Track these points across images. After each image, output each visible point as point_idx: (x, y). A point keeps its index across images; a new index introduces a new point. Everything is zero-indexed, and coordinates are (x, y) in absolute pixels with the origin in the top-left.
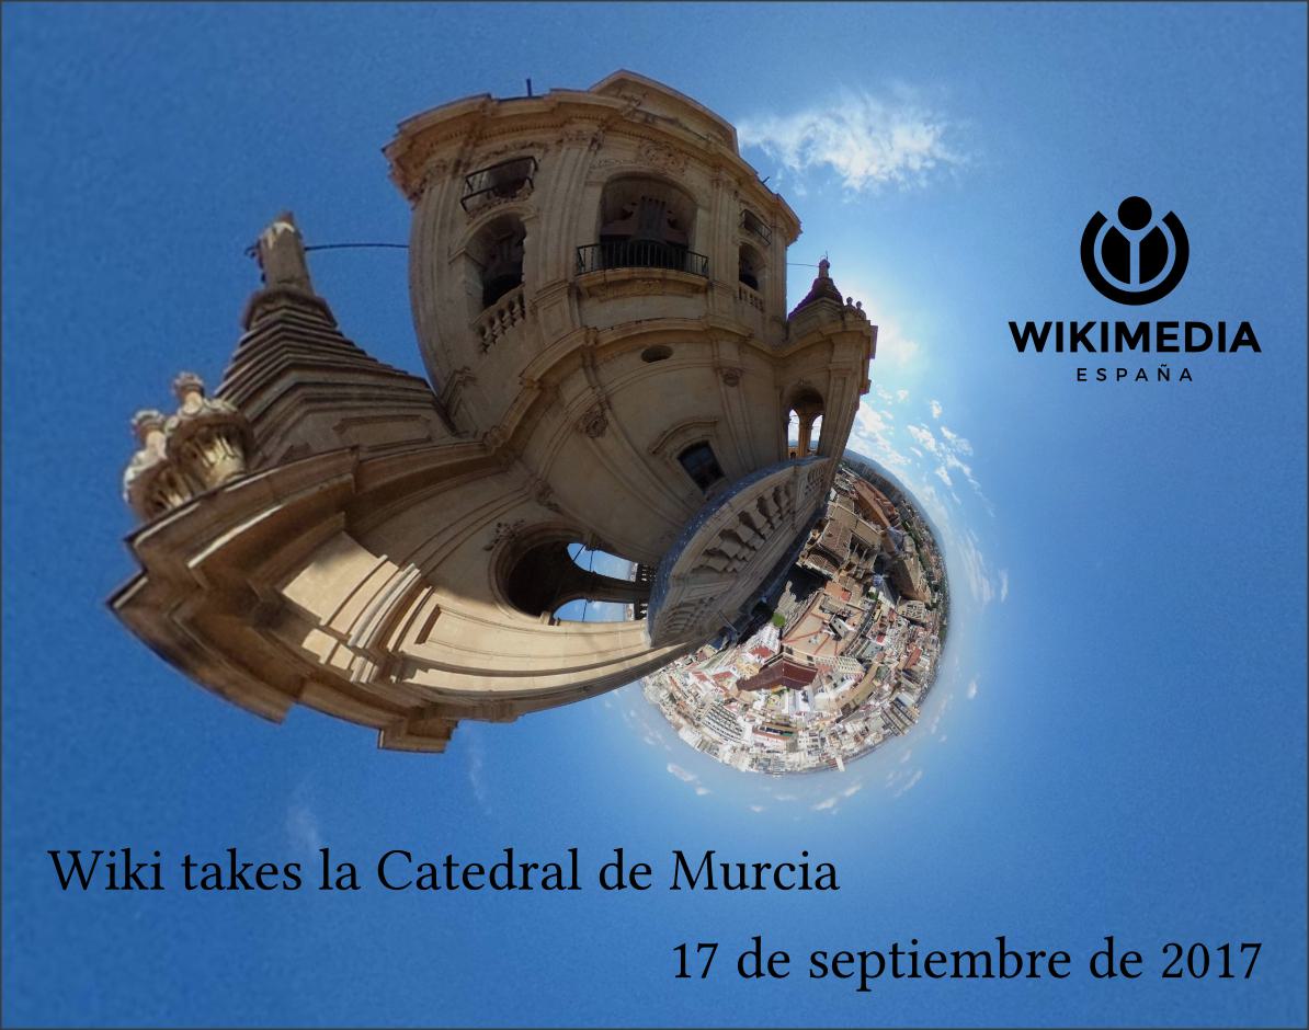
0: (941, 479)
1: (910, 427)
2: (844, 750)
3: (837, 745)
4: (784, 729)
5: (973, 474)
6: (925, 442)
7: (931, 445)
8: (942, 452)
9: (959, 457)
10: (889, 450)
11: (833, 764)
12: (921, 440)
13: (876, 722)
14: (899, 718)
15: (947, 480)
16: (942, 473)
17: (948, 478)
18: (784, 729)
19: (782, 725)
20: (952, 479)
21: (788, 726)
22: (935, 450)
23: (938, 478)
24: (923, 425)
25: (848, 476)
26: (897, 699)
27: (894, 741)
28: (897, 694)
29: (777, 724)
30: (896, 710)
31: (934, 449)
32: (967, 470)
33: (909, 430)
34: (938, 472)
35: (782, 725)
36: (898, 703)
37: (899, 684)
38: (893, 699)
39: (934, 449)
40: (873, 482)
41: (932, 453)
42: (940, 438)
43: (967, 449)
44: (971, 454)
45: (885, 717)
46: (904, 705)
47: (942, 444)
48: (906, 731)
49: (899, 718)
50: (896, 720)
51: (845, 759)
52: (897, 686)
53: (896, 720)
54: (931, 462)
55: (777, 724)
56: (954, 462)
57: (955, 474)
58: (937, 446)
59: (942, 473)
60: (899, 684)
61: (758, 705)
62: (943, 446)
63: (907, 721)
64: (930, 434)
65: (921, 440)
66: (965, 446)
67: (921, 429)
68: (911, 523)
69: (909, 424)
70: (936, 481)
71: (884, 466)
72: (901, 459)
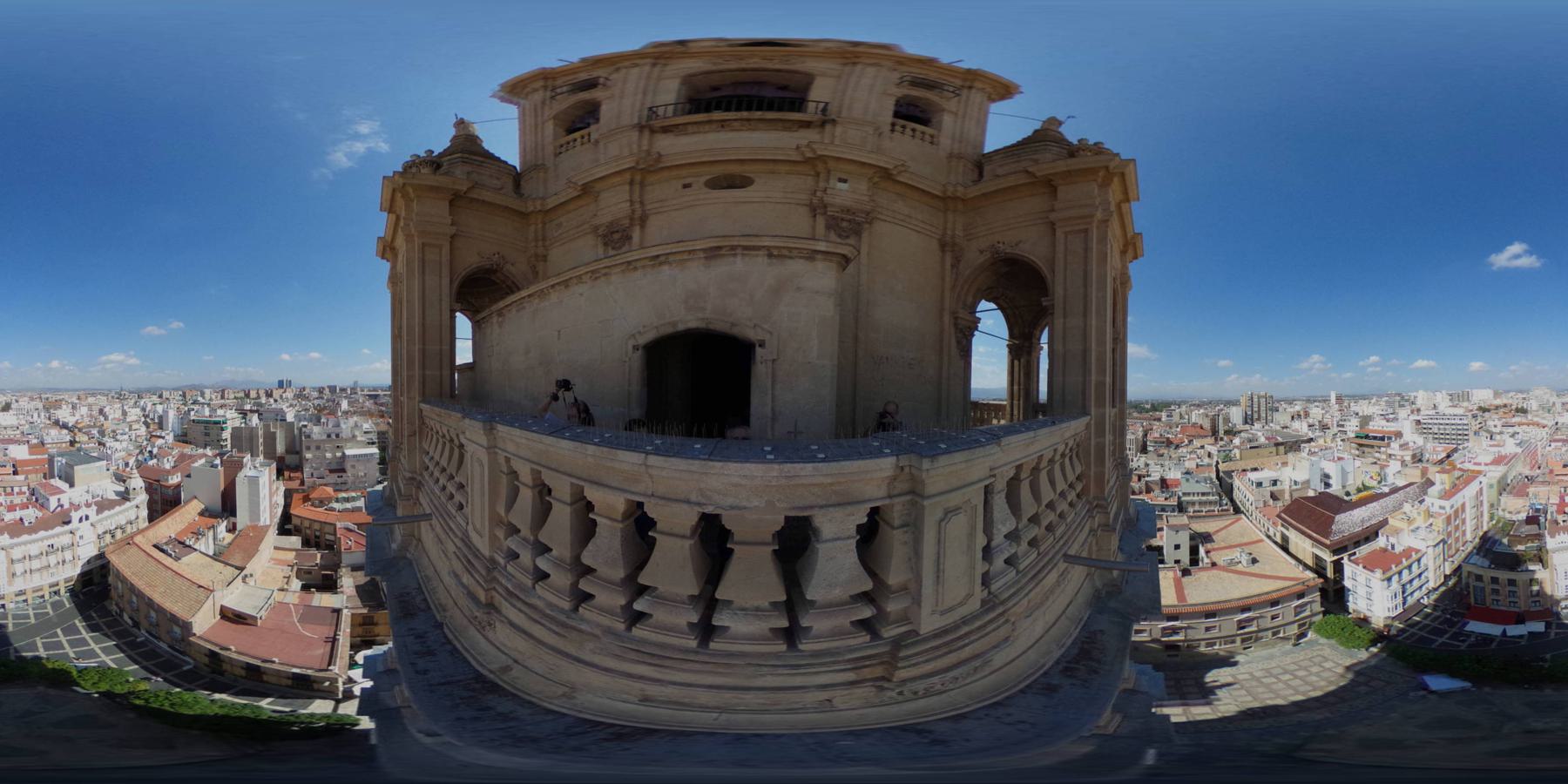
2: (1323, 409)
3: (1327, 416)
4: (1367, 441)
11: (1339, 399)
13: (1282, 418)
14: (1259, 407)
18: (1367, 441)
19: (1367, 446)
21: (1361, 445)
26: (1246, 422)
27: (1277, 395)
28: (1240, 427)
29: (1372, 447)
30: (1256, 416)
35: (1367, 446)
36: (1248, 420)
37: (1227, 432)
38: (1247, 427)
45: (1269, 418)
46: (1246, 413)
48: (1263, 393)
49: (1259, 407)
50: (1263, 408)
51: (1326, 400)
52: (1231, 433)
53: (1263, 408)
55: (1372, 447)
60: (1227, 432)
61: (1394, 466)
63: (1255, 400)
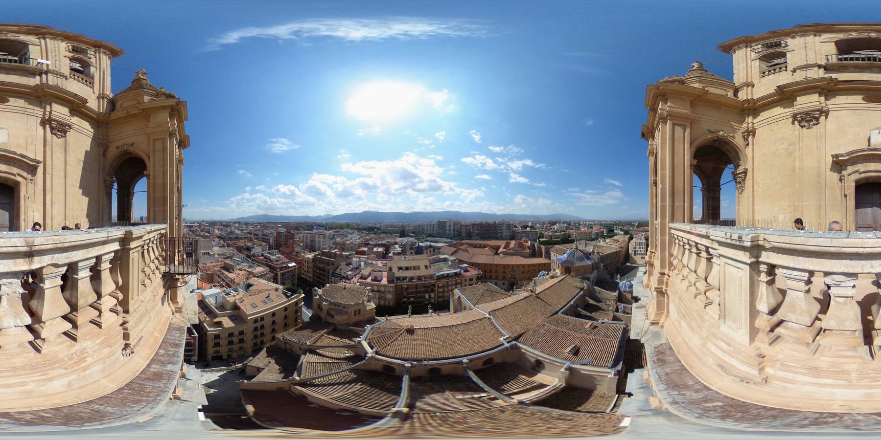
0: (518, 182)
1: (464, 160)
5: (534, 161)
6: (484, 165)
7: (490, 164)
8: (502, 163)
9: (520, 158)
10: (458, 190)
12: (480, 165)
15: (522, 180)
16: (515, 178)
17: (522, 178)
20: (526, 178)
22: (496, 166)
23: (517, 184)
24: (473, 152)
25: (437, 250)
31: (494, 166)
32: (529, 162)
33: (464, 163)
34: (512, 181)
39: (494, 166)
40: (469, 236)
41: (496, 169)
42: (493, 155)
43: (517, 151)
44: (522, 151)
47: (497, 158)
54: (501, 177)
56: (517, 165)
57: (525, 172)
58: (495, 162)
59: (515, 178)
62: (500, 160)
64: (484, 157)
65: (480, 165)
66: (514, 149)
67: (473, 156)
68: (542, 236)
69: (461, 159)
70: (518, 188)
71: (463, 210)
72: (476, 193)
